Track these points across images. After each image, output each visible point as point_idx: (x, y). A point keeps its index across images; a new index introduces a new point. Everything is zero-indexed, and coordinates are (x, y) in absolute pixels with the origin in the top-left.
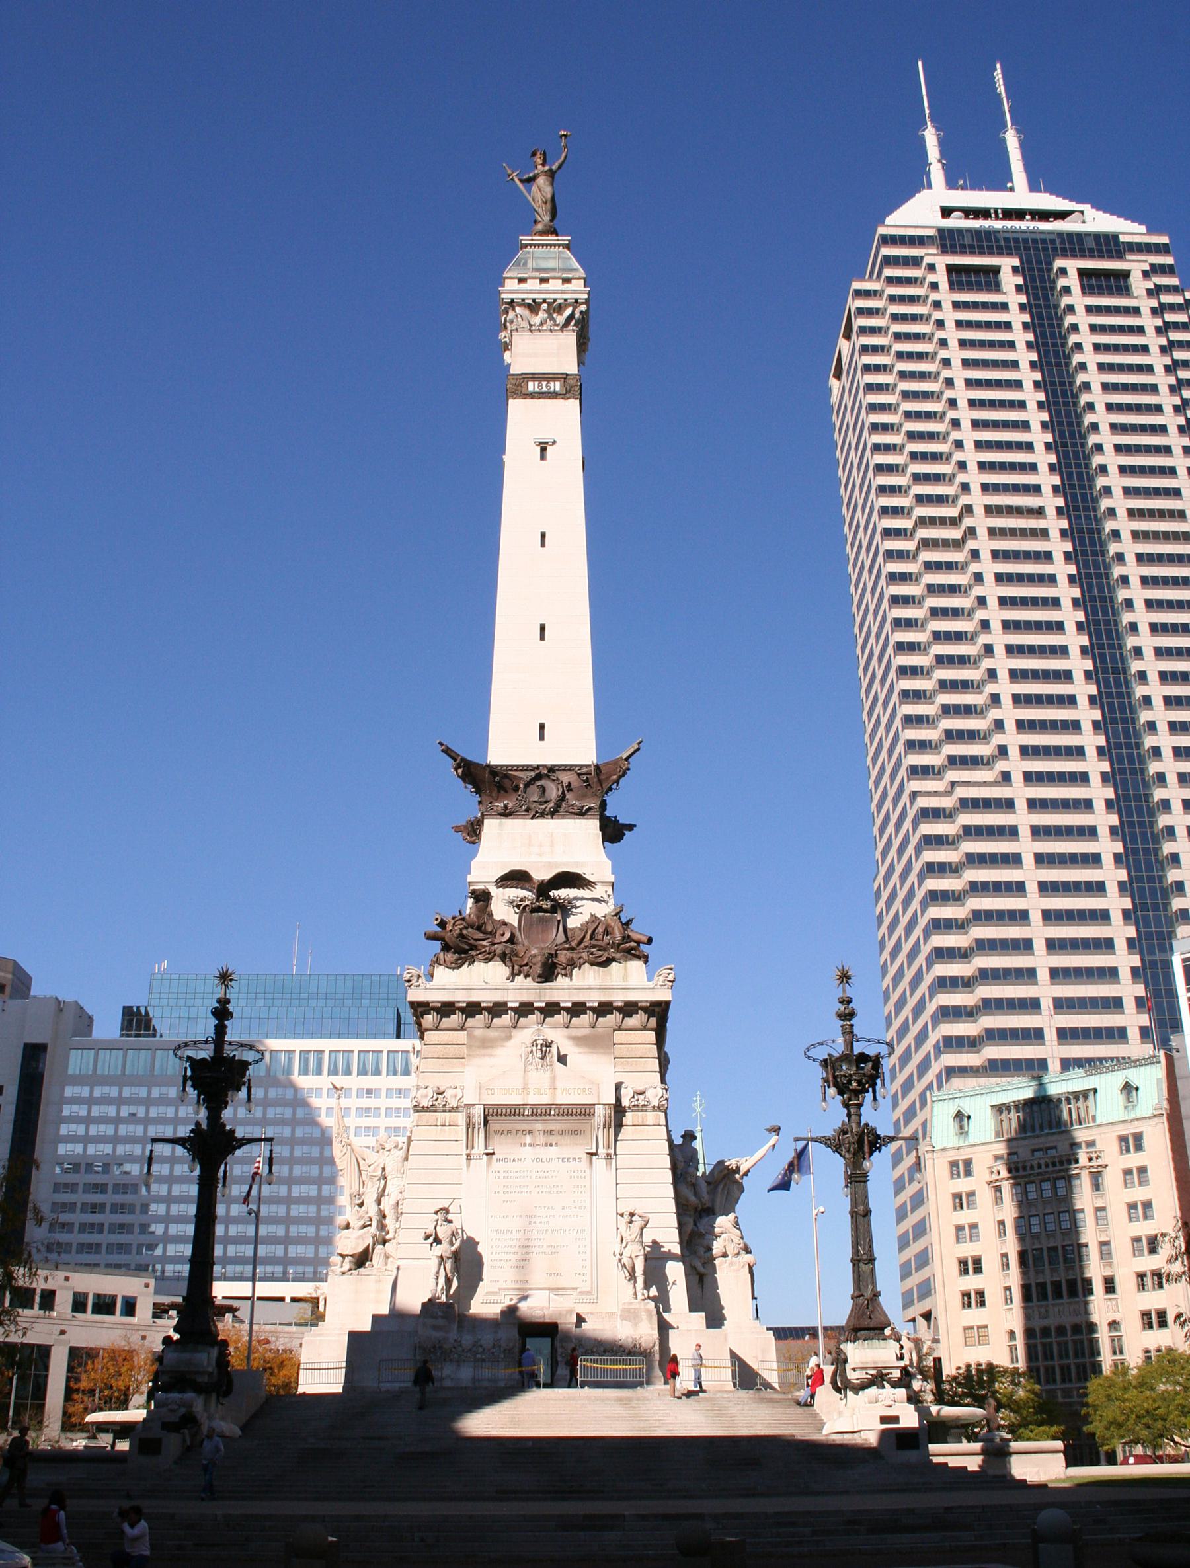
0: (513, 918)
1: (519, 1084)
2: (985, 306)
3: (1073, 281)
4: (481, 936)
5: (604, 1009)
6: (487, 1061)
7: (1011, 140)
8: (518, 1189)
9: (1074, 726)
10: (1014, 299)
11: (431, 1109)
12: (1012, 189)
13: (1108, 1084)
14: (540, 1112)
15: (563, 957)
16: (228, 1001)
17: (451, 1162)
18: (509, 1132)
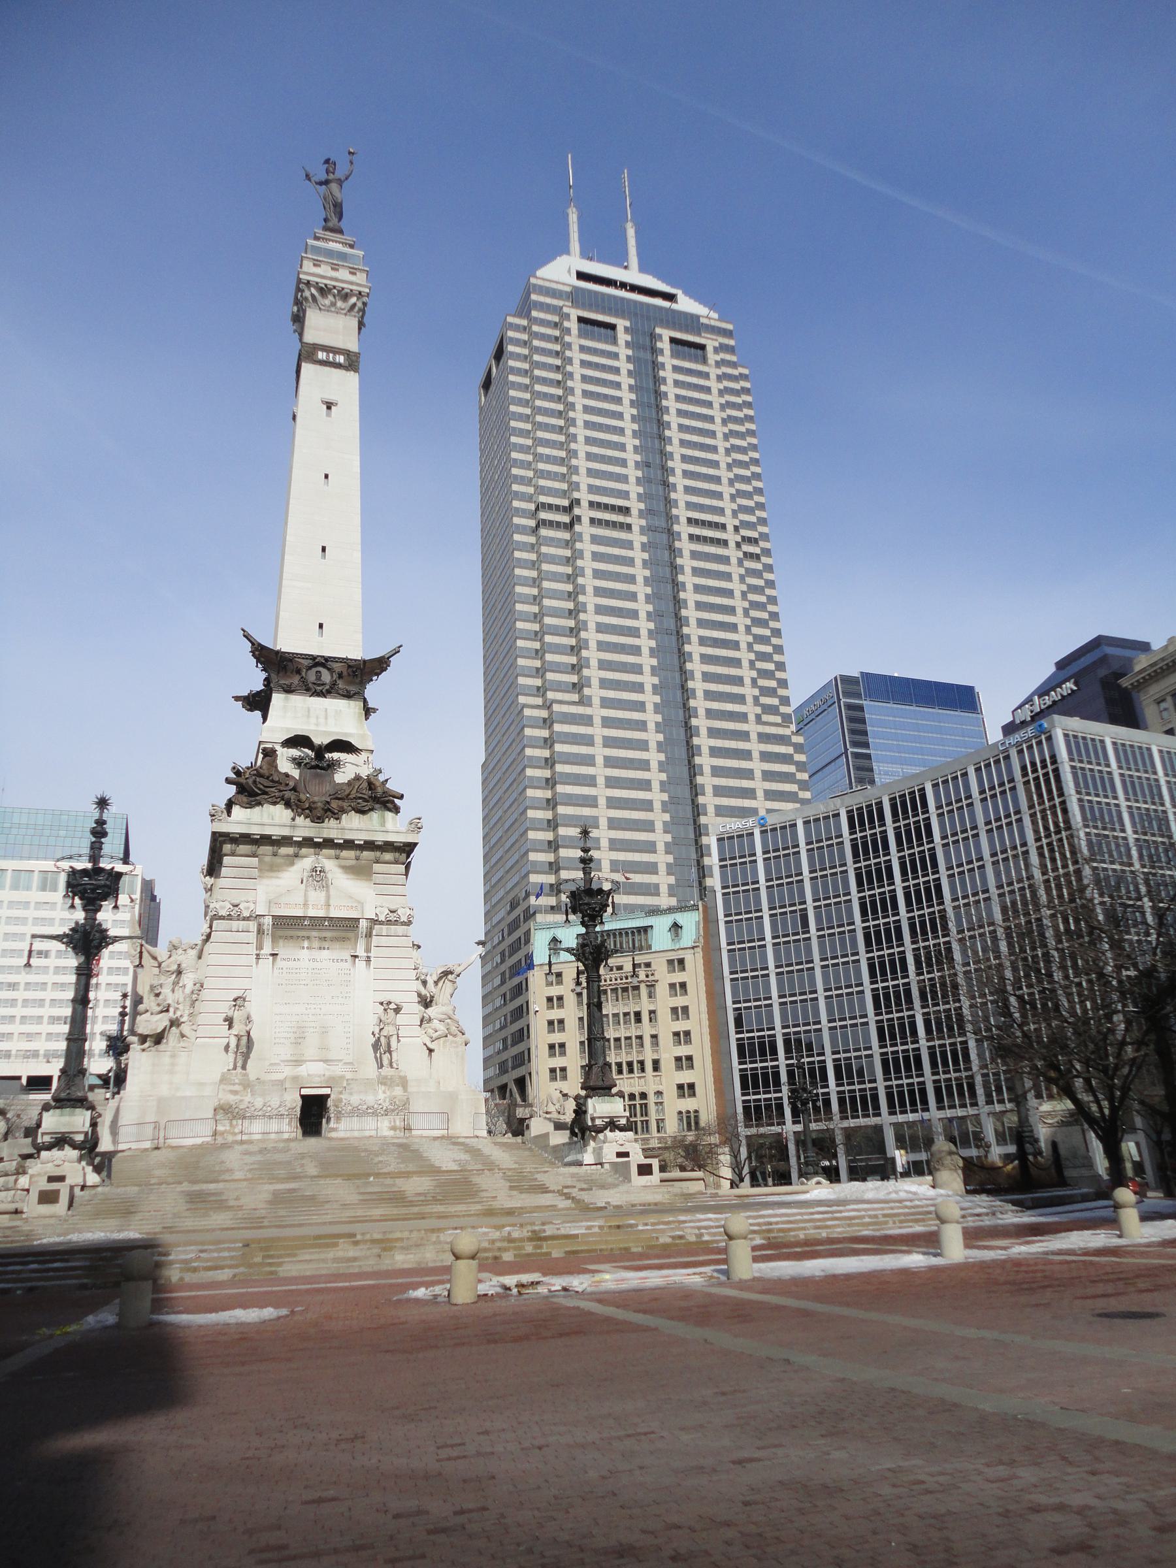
0: (295, 773)
1: (301, 900)
2: (603, 353)
3: (665, 345)
4: (271, 784)
5: (370, 845)
6: (275, 881)
9: (637, 669)
11: (229, 917)
12: (626, 268)
13: (661, 924)
14: (316, 923)
15: (334, 805)
16: (104, 823)
17: (243, 960)
18: (292, 937)
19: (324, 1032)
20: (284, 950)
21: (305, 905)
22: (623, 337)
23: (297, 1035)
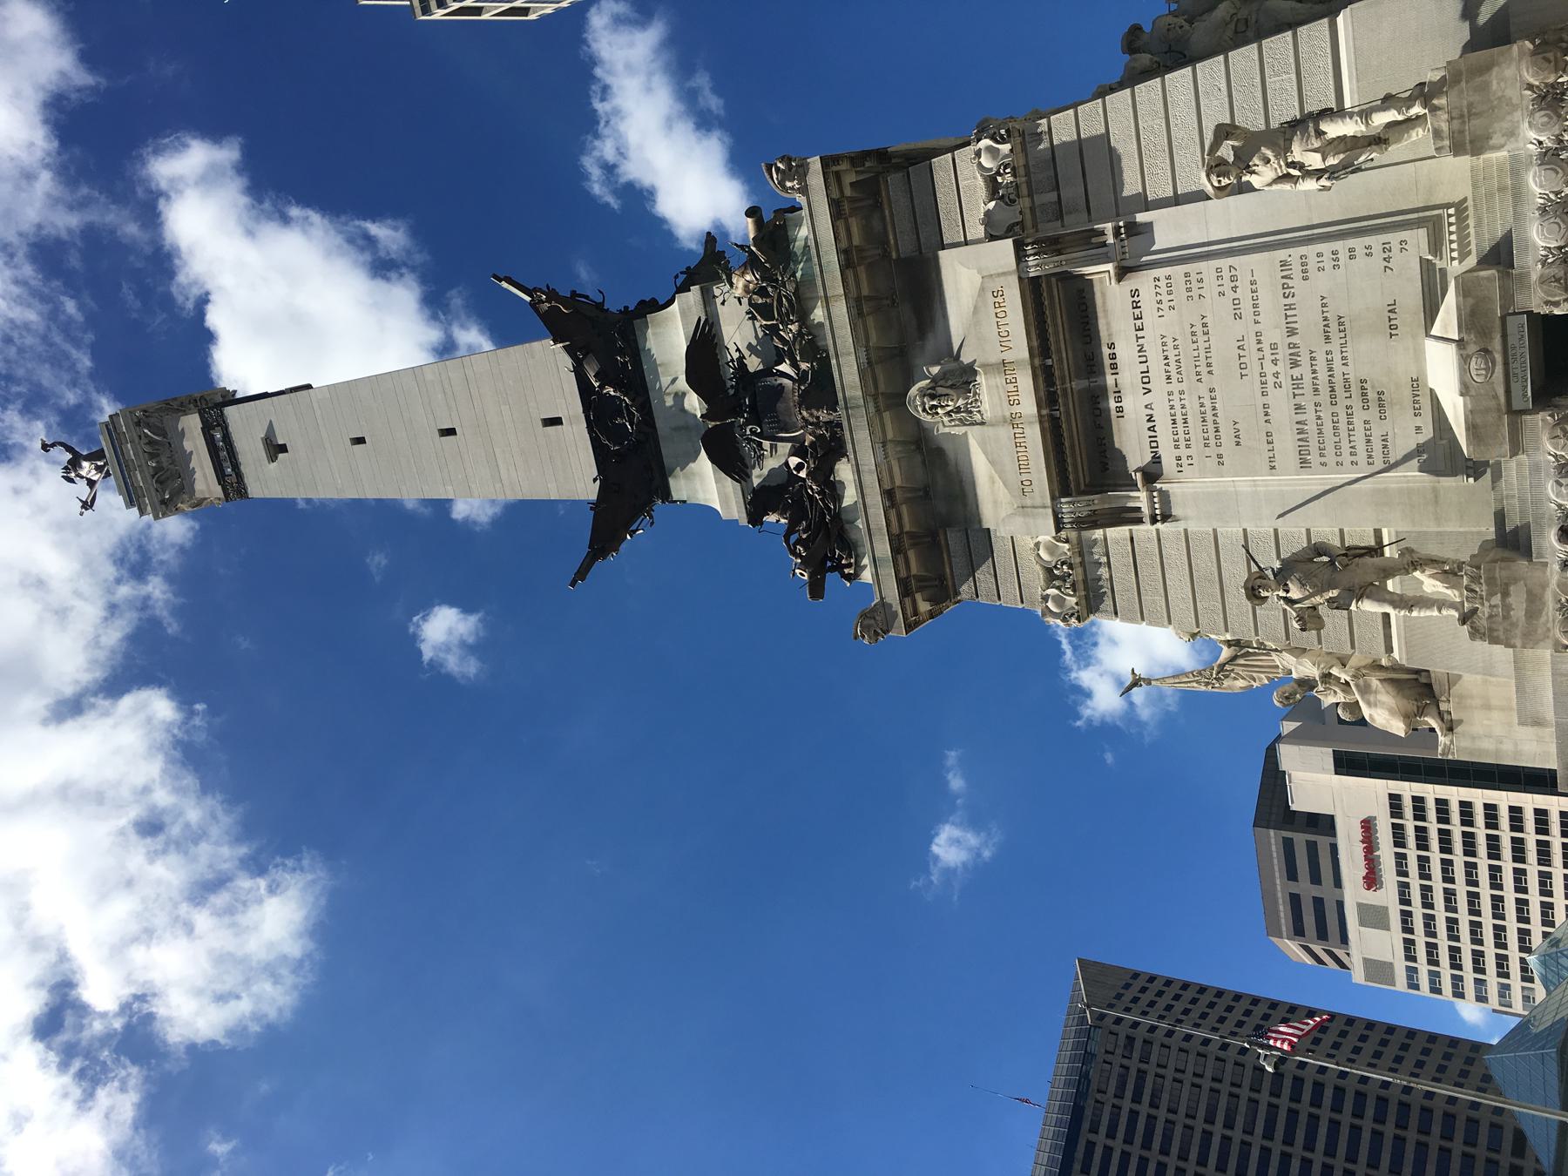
1: (1005, 433)
8: (1209, 418)
19: (1335, 327)
23: (1356, 402)
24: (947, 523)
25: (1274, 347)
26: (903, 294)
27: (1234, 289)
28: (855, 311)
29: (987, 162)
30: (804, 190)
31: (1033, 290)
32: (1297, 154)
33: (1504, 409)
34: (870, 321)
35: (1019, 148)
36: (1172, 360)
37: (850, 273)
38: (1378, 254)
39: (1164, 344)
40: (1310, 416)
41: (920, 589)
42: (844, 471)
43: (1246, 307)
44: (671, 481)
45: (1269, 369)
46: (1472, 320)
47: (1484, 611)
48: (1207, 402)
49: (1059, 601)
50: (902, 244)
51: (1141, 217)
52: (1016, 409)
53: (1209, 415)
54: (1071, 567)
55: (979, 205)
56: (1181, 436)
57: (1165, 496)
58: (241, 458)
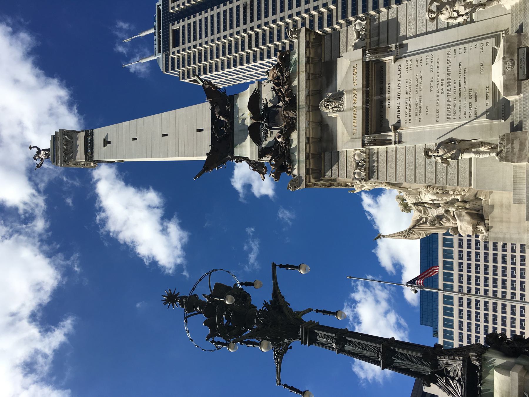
1: (350, 113)
2: (184, 33)
7: (143, 34)
8: (418, 106)
10: (182, 23)
19: (463, 72)
20: (391, 119)
21: (353, 109)
22: (176, 26)
23: (467, 97)
24: (325, 150)
25: (442, 80)
26: (323, 71)
27: (432, 62)
28: (307, 77)
29: (358, 27)
30: (298, 38)
31: (366, 65)
32: (457, 7)
33: (516, 78)
34: (312, 82)
35: (368, 24)
36: (408, 88)
37: (308, 49)
38: (479, 47)
39: (406, 82)
40: (451, 103)
41: (312, 173)
42: (294, 136)
43: (435, 68)
44: (235, 149)
45: (440, 87)
46: (508, 51)
47: (505, 150)
48: (418, 101)
49: (359, 174)
50: (326, 57)
51: (404, 42)
52: (355, 105)
53: (419, 106)
54: (365, 162)
55: (353, 39)
56: (408, 113)
57: (400, 134)
58: (94, 147)
